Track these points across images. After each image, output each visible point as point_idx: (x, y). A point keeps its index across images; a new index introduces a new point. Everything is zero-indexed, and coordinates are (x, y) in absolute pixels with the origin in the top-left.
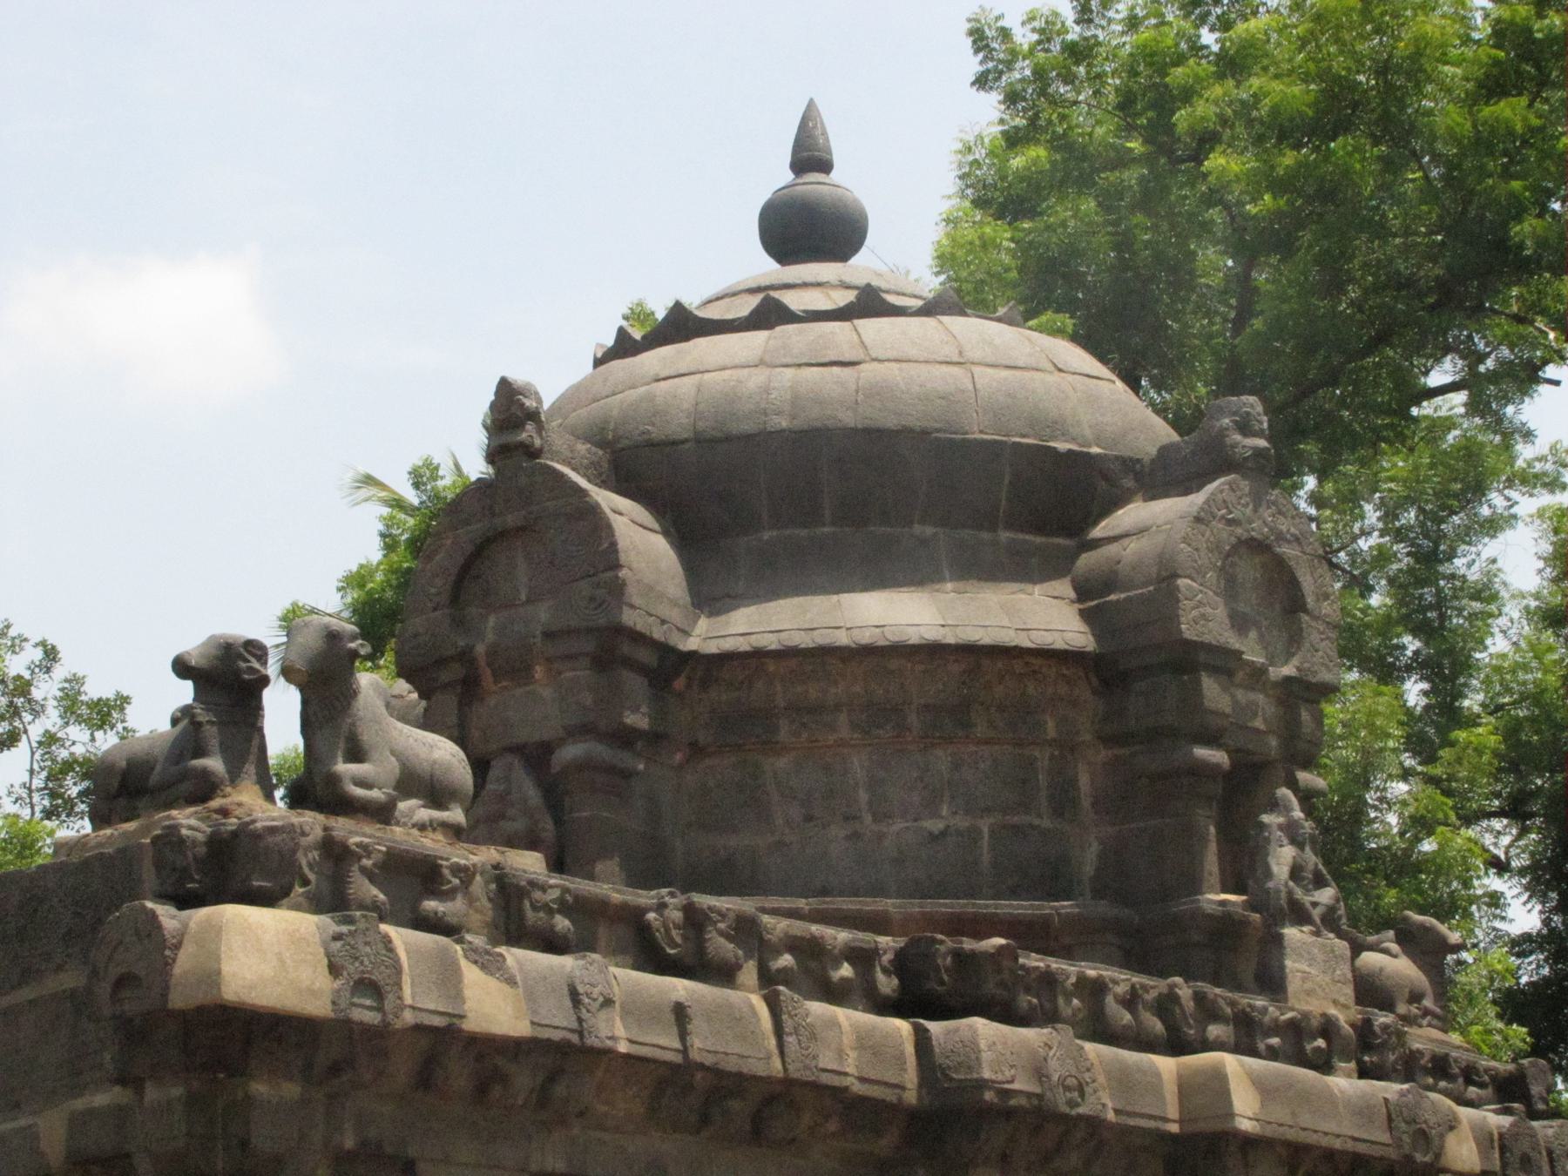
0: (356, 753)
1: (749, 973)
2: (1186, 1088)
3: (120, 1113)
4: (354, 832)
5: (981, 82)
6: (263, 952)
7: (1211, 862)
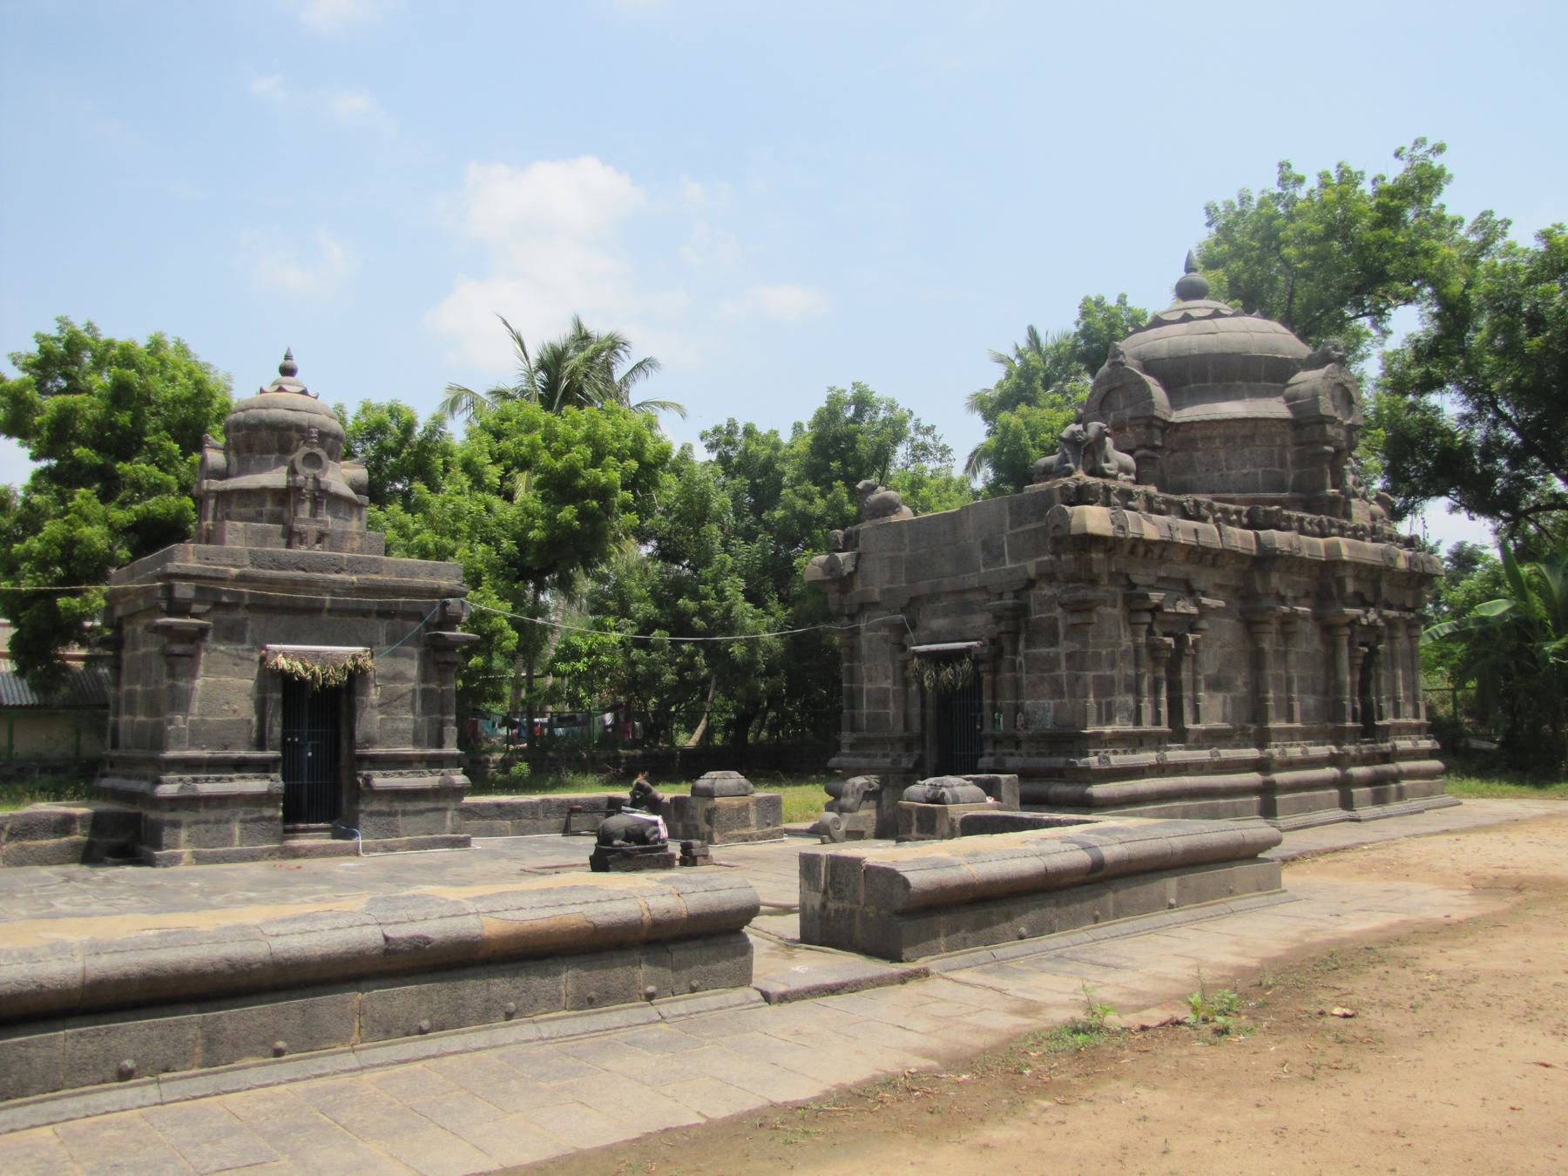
0: (1107, 461)
1: (1211, 520)
2: (1327, 548)
3: (1051, 562)
4: (1111, 484)
5: (1209, 225)
6: (1095, 519)
7: (1329, 481)
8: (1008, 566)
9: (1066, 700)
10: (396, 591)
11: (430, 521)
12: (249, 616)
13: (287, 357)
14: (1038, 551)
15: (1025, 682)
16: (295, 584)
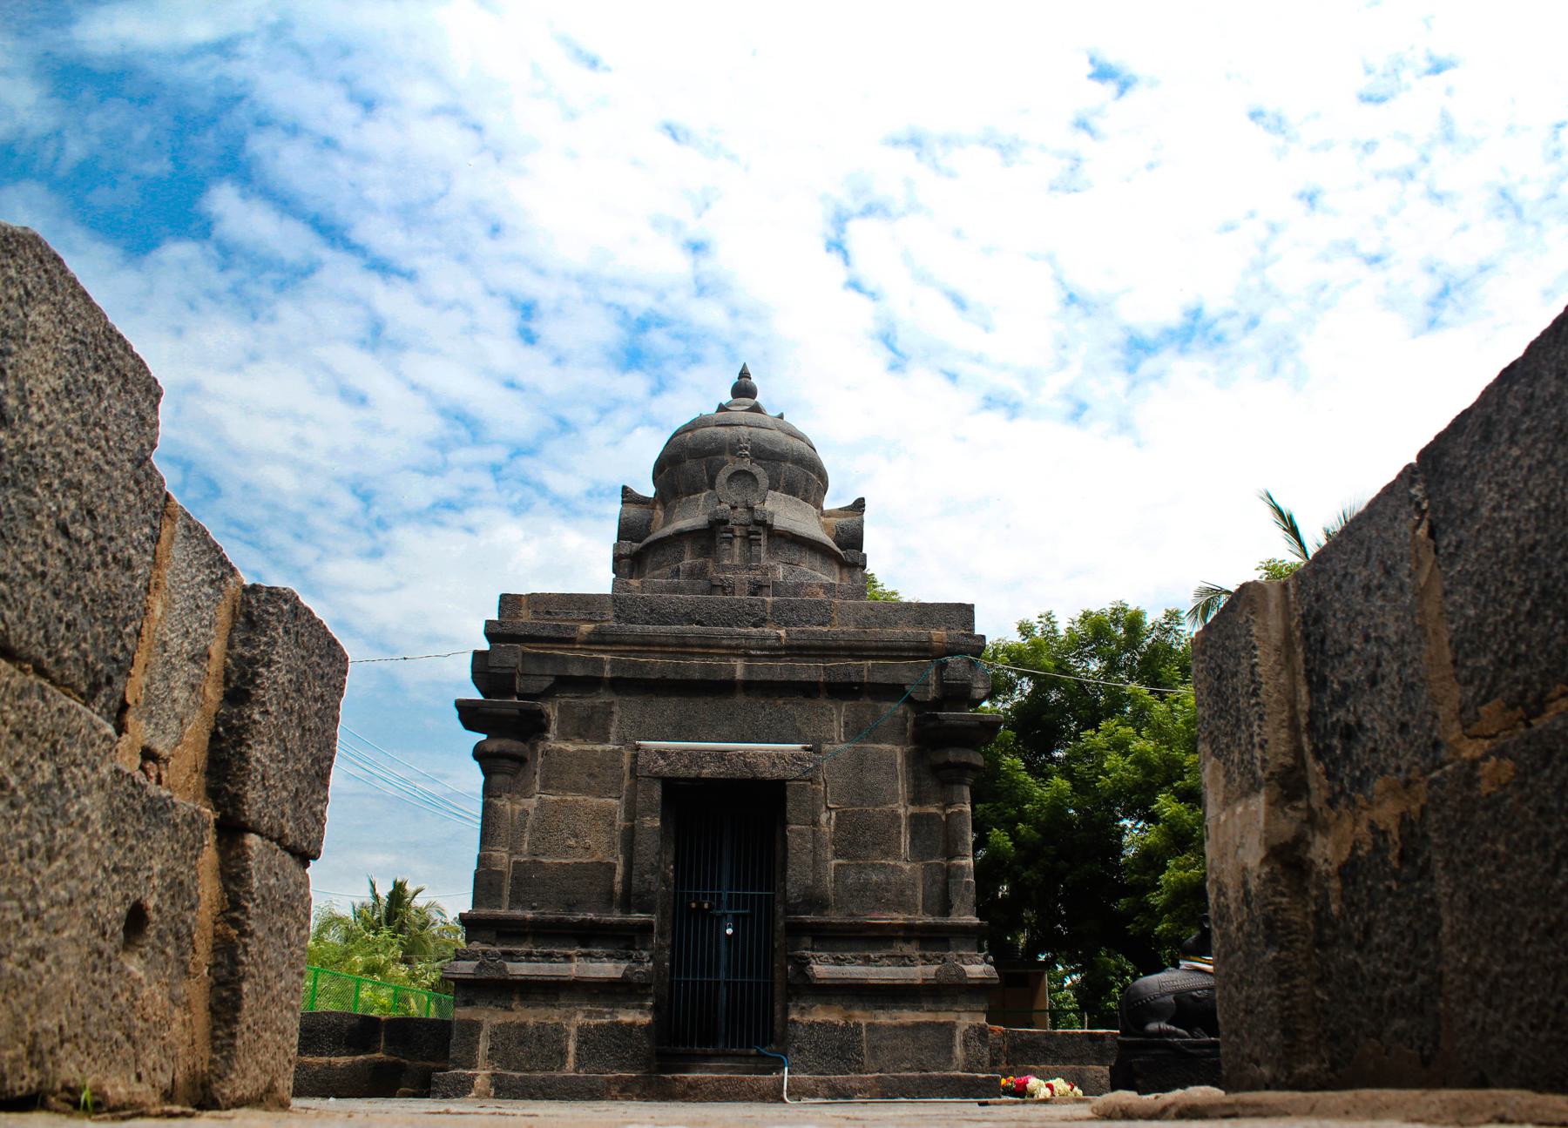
10: (856, 651)
11: (1159, 733)
12: (616, 699)
13: (744, 374)
16: (682, 646)
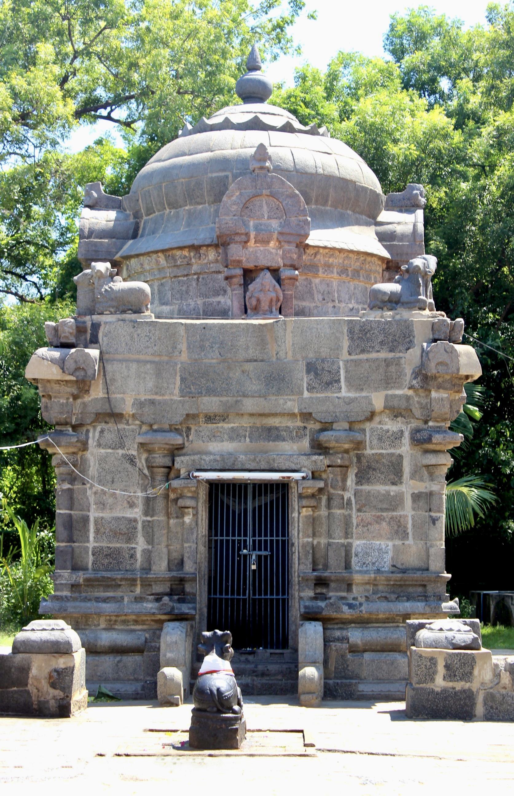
8: (344, 393)
9: (410, 541)
14: (388, 382)
15: (355, 521)
